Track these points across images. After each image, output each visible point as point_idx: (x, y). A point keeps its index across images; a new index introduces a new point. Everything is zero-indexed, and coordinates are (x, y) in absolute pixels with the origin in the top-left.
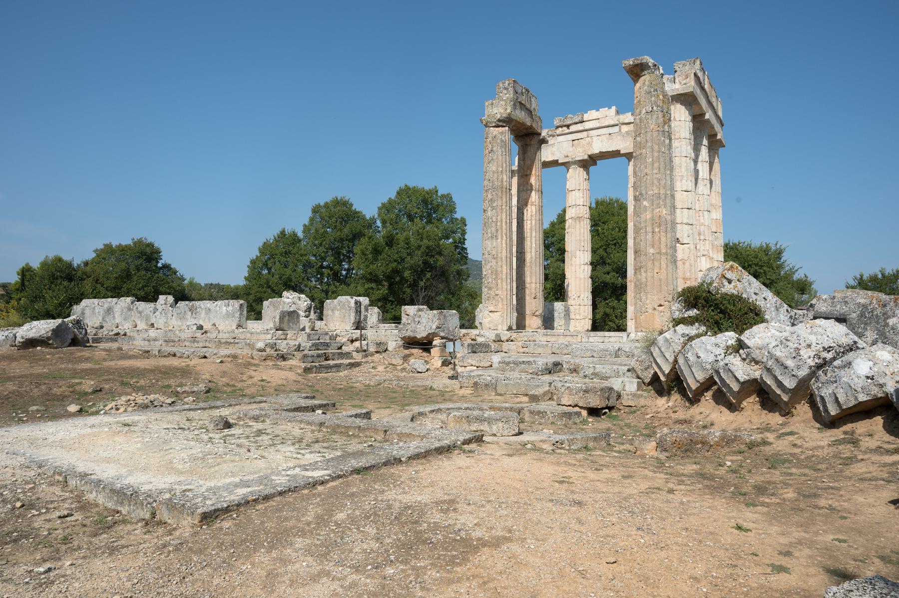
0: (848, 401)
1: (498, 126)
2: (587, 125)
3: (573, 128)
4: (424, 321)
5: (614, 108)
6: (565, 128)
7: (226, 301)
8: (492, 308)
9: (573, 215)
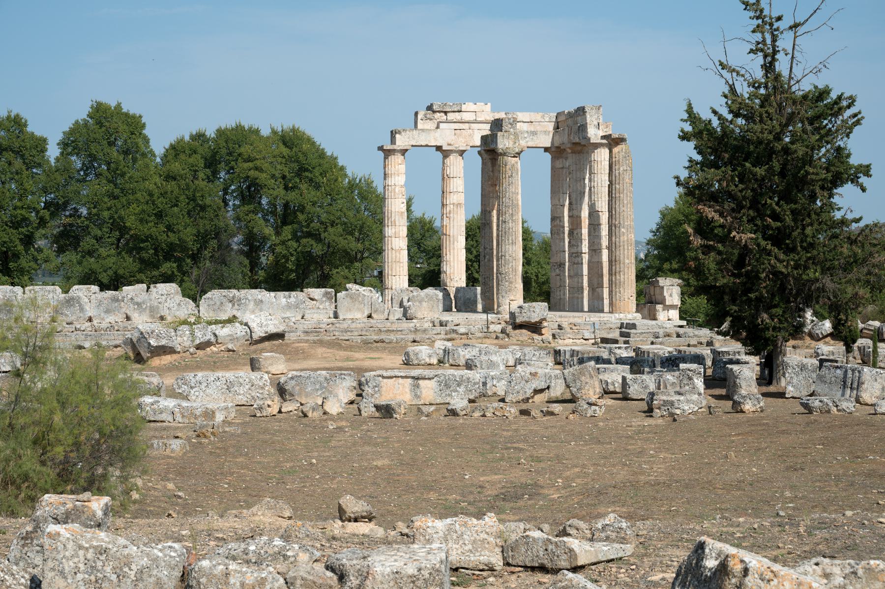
0: (825, 333)
1: (514, 157)
2: (466, 117)
3: (451, 116)
4: (537, 310)
5: (489, 104)
6: (443, 114)
7: (287, 293)
8: (512, 298)
9: (455, 201)
